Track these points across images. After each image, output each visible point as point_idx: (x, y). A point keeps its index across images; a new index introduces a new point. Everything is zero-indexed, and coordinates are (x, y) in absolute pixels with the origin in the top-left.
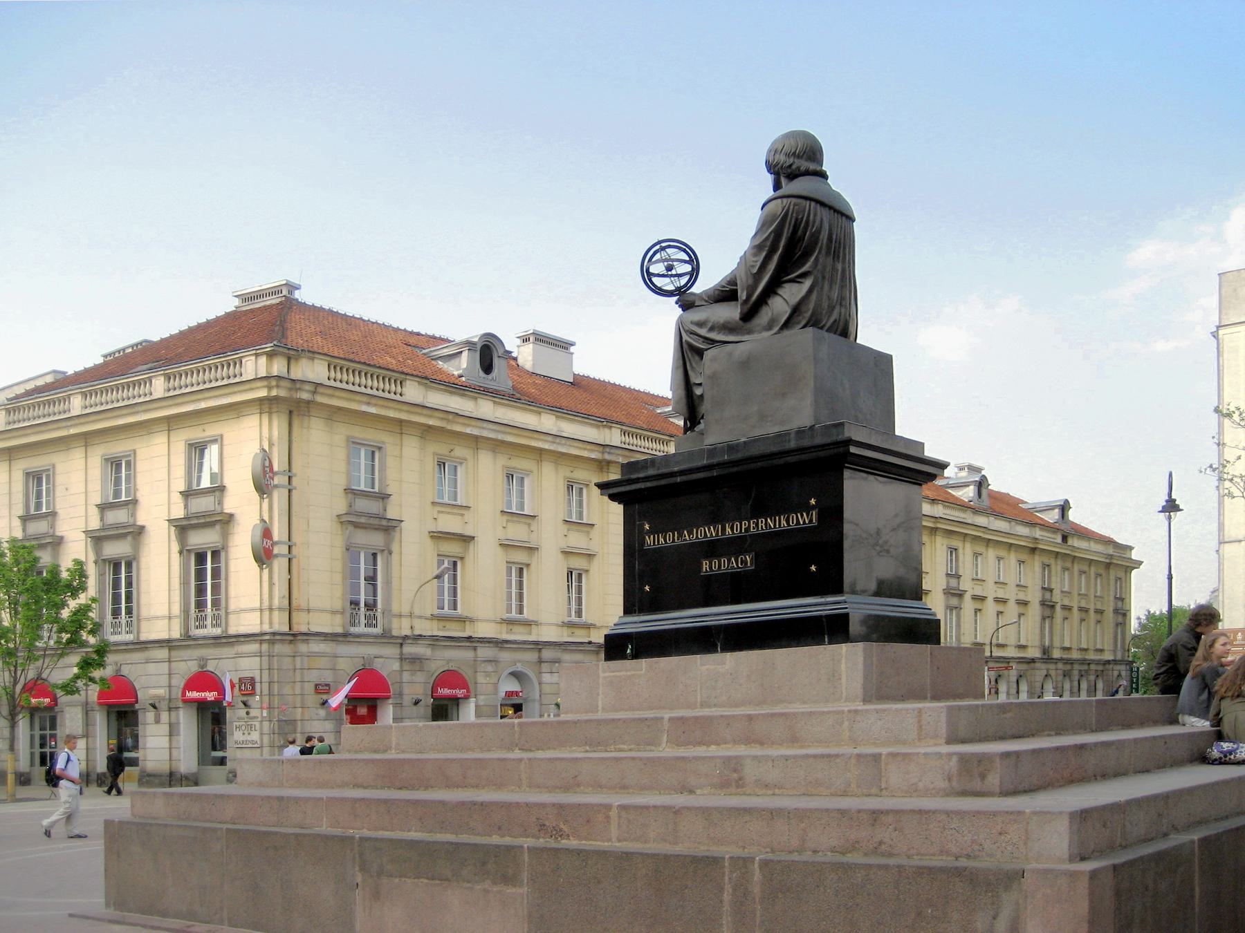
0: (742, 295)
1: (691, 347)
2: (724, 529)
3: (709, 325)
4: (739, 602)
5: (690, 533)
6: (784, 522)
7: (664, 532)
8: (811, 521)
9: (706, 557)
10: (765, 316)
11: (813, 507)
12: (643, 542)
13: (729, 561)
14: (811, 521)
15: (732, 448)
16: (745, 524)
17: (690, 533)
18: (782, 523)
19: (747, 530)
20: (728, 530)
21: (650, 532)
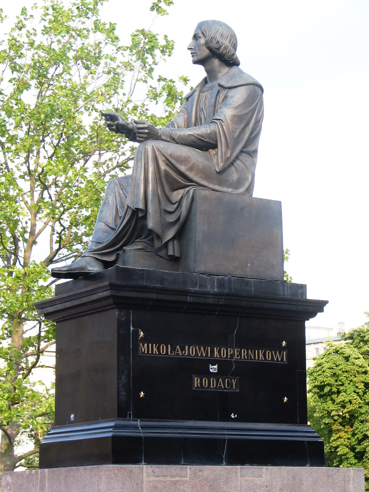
2: (212, 352)
5: (183, 349)
7: (159, 343)
8: (282, 359)
17: (183, 349)
18: (260, 355)
19: (232, 356)
20: (216, 353)
21: (144, 340)
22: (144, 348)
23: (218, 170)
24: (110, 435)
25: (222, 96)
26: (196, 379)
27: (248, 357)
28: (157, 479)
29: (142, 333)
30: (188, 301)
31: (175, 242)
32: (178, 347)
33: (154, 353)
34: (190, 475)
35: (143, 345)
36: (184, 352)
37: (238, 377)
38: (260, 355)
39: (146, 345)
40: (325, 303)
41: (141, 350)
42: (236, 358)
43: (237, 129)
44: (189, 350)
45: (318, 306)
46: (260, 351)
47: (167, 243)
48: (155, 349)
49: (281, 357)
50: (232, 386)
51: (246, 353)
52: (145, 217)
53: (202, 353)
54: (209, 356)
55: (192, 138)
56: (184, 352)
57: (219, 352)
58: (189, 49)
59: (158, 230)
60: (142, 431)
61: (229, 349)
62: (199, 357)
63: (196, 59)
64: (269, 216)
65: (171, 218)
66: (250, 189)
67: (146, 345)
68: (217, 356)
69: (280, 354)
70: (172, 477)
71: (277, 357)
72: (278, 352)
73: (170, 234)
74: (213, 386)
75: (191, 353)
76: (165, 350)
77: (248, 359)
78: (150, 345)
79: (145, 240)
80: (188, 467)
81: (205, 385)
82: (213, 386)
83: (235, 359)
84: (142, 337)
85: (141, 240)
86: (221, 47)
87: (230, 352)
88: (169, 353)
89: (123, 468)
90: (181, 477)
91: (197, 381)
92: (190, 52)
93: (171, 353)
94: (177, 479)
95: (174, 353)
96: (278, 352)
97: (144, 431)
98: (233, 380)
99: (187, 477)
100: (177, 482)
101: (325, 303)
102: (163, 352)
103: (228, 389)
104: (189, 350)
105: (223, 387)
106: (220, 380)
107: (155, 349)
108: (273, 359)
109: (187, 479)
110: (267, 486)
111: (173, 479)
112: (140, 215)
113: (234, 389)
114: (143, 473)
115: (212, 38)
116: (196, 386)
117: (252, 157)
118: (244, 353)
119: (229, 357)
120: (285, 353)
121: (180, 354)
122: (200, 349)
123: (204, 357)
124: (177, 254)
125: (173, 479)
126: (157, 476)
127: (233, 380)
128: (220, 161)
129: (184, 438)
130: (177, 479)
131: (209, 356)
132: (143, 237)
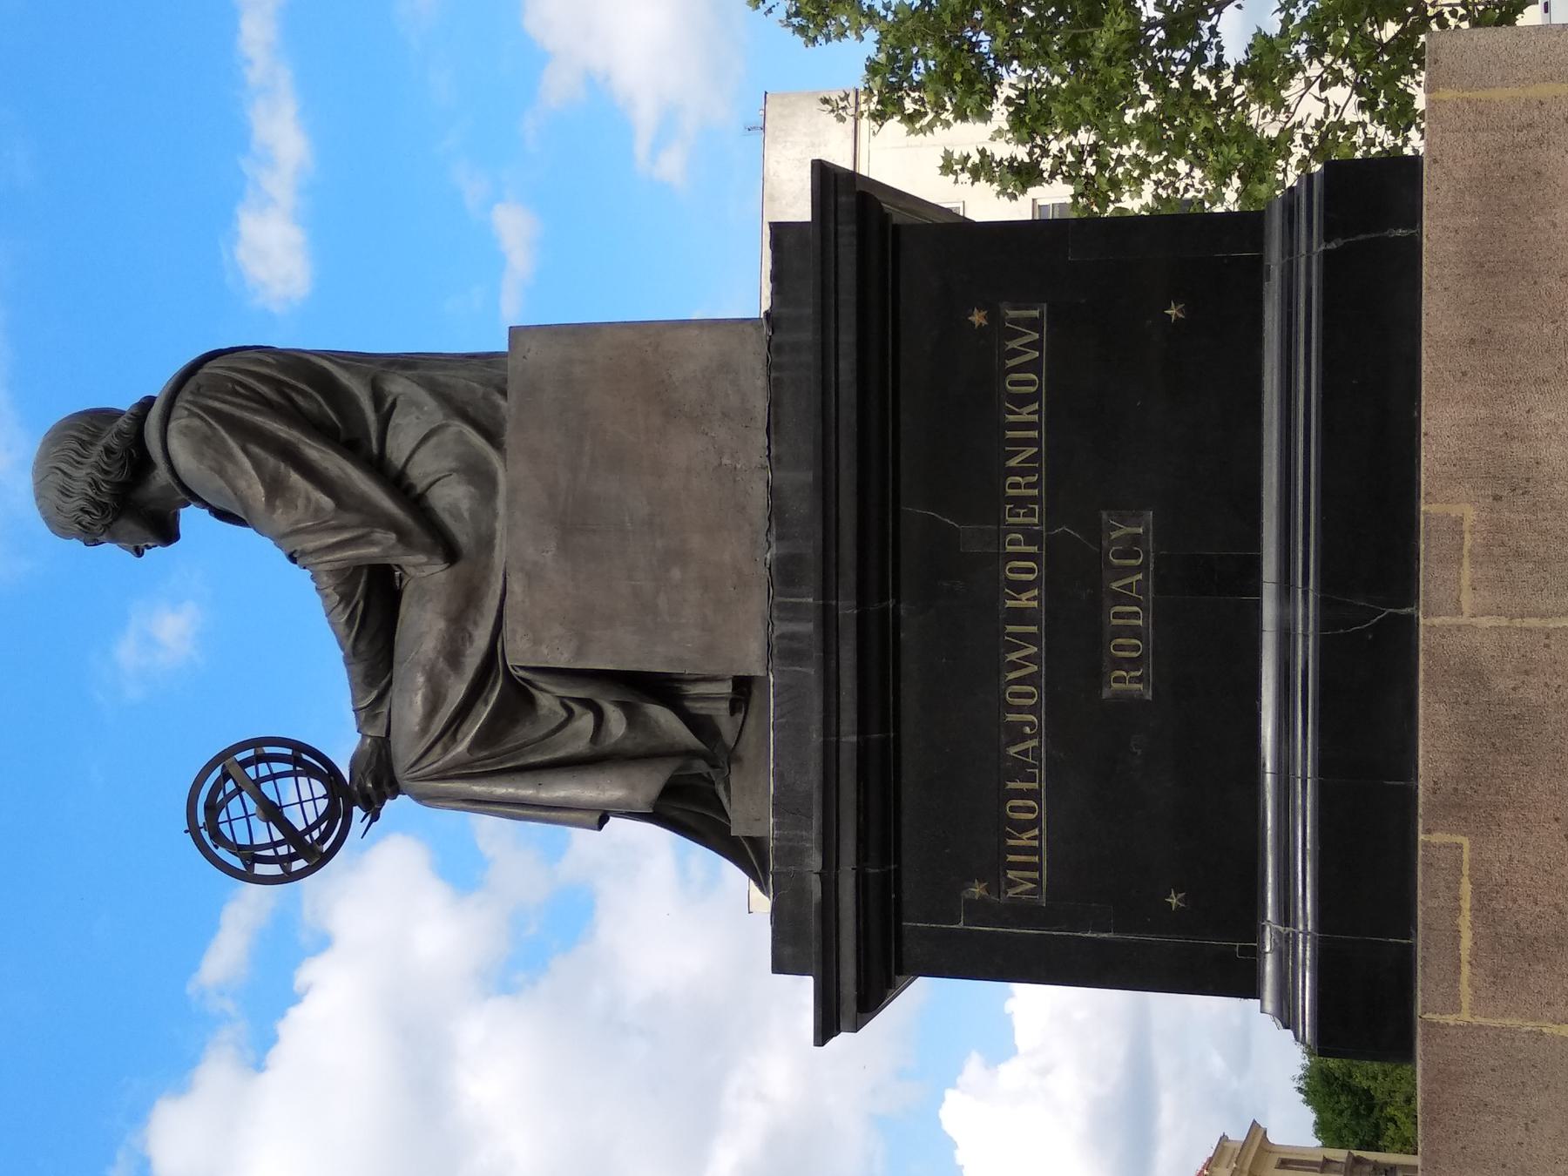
0: (379, 547)
1: (486, 738)
2: (1020, 616)
3: (441, 664)
4: (1255, 564)
6: (1026, 415)
7: (1005, 826)
8: (1033, 324)
9: (1097, 677)
10: (452, 498)
11: (994, 316)
12: (1022, 912)
13: (1119, 598)
14: (1033, 324)
15: (784, 574)
16: (1016, 544)
19: (1031, 537)
20: (1026, 601)
21: (995, 879)
22: (1022, 885)
26: (1115, 686)
27: (1031, 472)
32: (1012, 751)
35: (1012, 884)
36: (1027, 730)
37: (1104, 515)
39: (1011, 874)
43: (308, 499)
44: (1019, 710)
46: (1011, 418)
48: (1025, 840)
50: (1136, 539)
53: (1026, 658)
54: (1033, 629)
55: (362, 647)
56: (1027, 730)
57: (1022, 587)
61: (1010, 548)
68: (1034, 598)
74: (1135, 615)
77: (1038, 471)
78: (1011, 858)
81: (1136, 648)
83: (1040, 523)
95: (1034, 766)
98: (1114, 535)
103: (1147, 553)
105: (1140, 577)
113: (1146, 532)
118: (1016, 486)
119: (1034, 549)
120: (1012, 314)
121: (1034, 743)
122: (1015, 666)
127: (1114, 535)
131: (1033, 629)
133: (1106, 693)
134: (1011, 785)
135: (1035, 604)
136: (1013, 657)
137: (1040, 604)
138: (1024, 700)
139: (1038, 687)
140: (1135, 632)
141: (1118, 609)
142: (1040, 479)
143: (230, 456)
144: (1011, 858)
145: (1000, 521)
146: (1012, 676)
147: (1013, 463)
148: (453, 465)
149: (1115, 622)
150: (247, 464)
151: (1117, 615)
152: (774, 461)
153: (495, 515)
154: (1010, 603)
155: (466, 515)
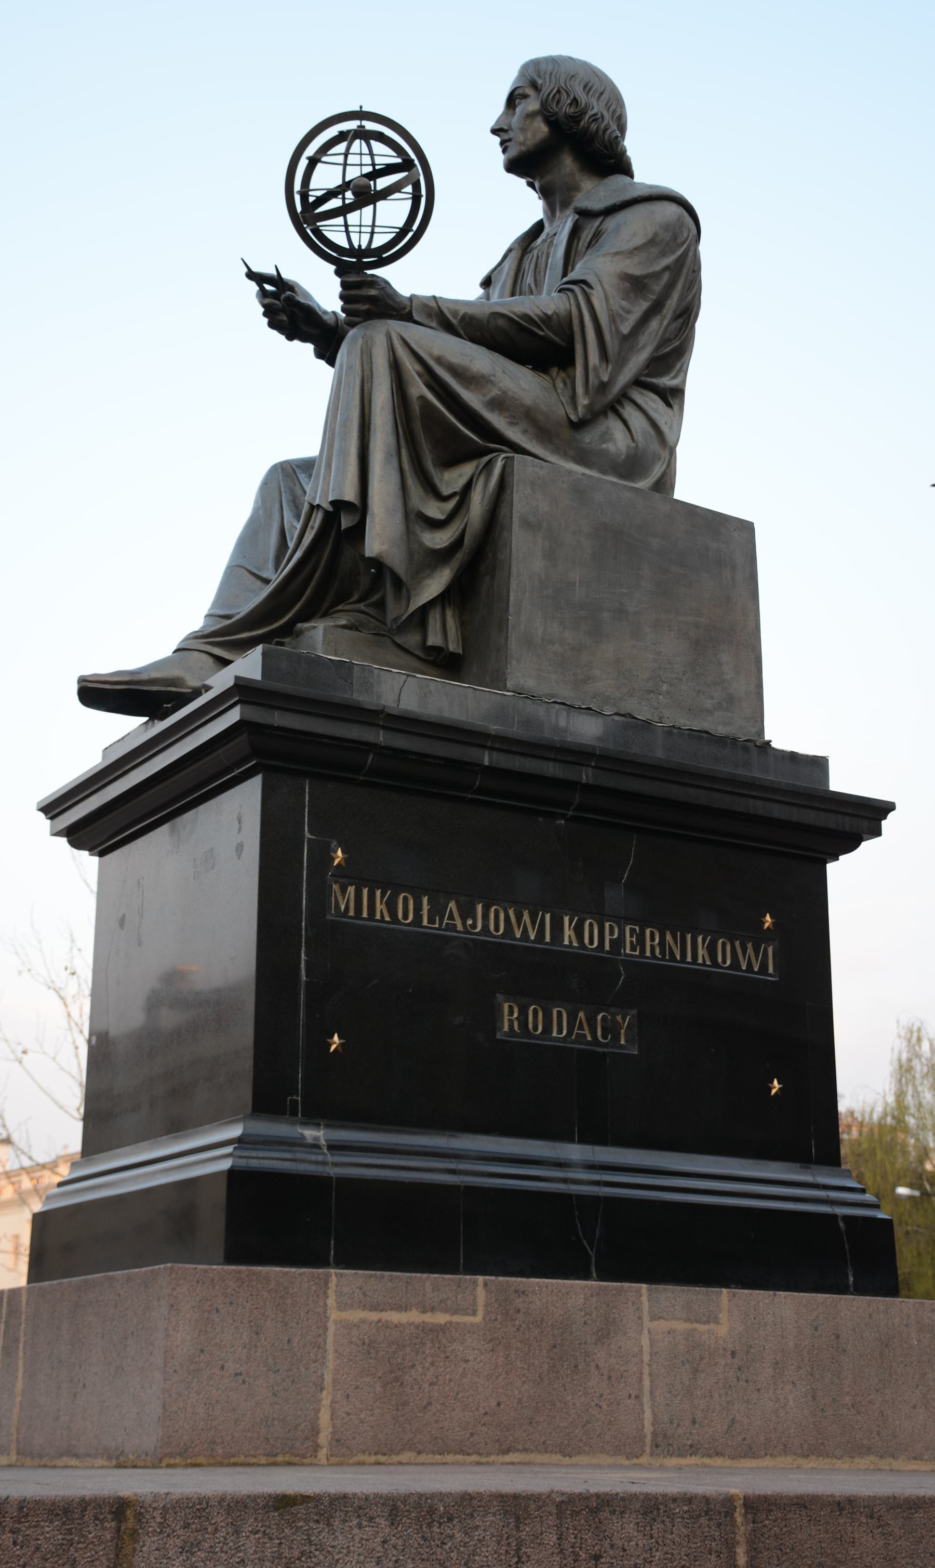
2: (557, 928)
3: (495, 392)
5: (467, 912)
7: (393, 886)
11: (767, 937)
13: (572, 1017)
17: (467, 912)
18: (698, 952)
19: (617, 944)
20: (568, 933)
21: (346, 875)
22: (344, 899)
23: (573, 418)
24: (226, 1165)
25: (586, 235)
26: (506, 1006)
27: (663, 952)
28: (374, 1316)
29: (339, 853)
30: (486, 763)
31: (449, 614)
32: (452, 905)
33: (378, 917)
34: (487, 1305)
35: (344, 890)
36: (470, 922)
37: (634, 1012)
38: (698, 952)
39: (351, 890)
40: (883, 809)
41: (337, 906)
42: (628, 951)
43: (628, 312)
44: (485, 917)
45: (864, 818)
46: (700, 939)
47: (424, 610)
49: (760, 962)
50: (616, 1038)
51: (657, 941)
52: (359, 531)
53: (525, 930)
54: (548, 939)
55: (501, 322)
56: (470, 922)
58: (495, 131)
59: (397, 561)
60: (330, 1158)
62: (516, 939)
63: (514, 151)
64: (722, 551)
65: (440, 539)
66: (665, 484)
67: (351, 890)
68: (571, 942)
69: (756, 951)
70: (424, 1311)
71: (749, 959)
72: (750, 946)
73: (434, 585)
74: (560, 1031)
75: (492, 927)
76: (410, 911)
77: (663, 959)
78: (365, 892)
79: (361, 606)
80: (481, 1279)
81: (536, 1029)
82: (560, 1031)
83: (626, 955)
84: (339, 864)
85: (348, 607)
86: (583, 113)
87: (612, 933)
88: (425, 923)
89: (254, 1273)
90: (455, 1312)
91: (511, 1013)
92: (497, 140)
93: (431, 920)
94: (442, 1318)
95: (441, 923)
96: (750, 946)
97: (337, 1159)
99: (474, 1313)
100: (443, 1328)
101: (883, 809)
102: (405, 916)
103: (605, 1045)
104: (485, 917)
105: (589, 1038)
106: (581, 1015)
107: (379, 907)
108: (735, 965)
109: (478, 1319)
110: (733, 1354)
111: (428, 1318)
112: (346, 522)
113: (622, 1047)
114: (325, 1293)
115: (558, 91)
116: (506, 1028)
117: (669, 405)
118: (653, 939)
119: (607, 947)
121: (460, 927)
122: (519, 918)
123: (533, 942)
124: (454, 646)
125: (428, 1318)
126: (375, 1308)
128: (580, 390)
129: (466, 1187)
130: (442, 1318)
131: (548, 939)
132: (355, 598)
133: (500, 997)
134: (425, 900)
135: (566, 942)
136: (526, 917)
137: (566, 946)
138: (493, 921)
139: (503, 936)
140: (547, 1029)
141: (565, 1015)
142: (658, 959)
143: (663, 254)
144: (365, 892)
145: (628, 920)
146: (511, 913)
147: (669, 937)
148: (640, 445)
149: (555, 1011)
150: (657, 267)
151: (560, 1014)
152: (672, 731)
153: (603, 472)
154: (566, 919)
155: (604, 446)
